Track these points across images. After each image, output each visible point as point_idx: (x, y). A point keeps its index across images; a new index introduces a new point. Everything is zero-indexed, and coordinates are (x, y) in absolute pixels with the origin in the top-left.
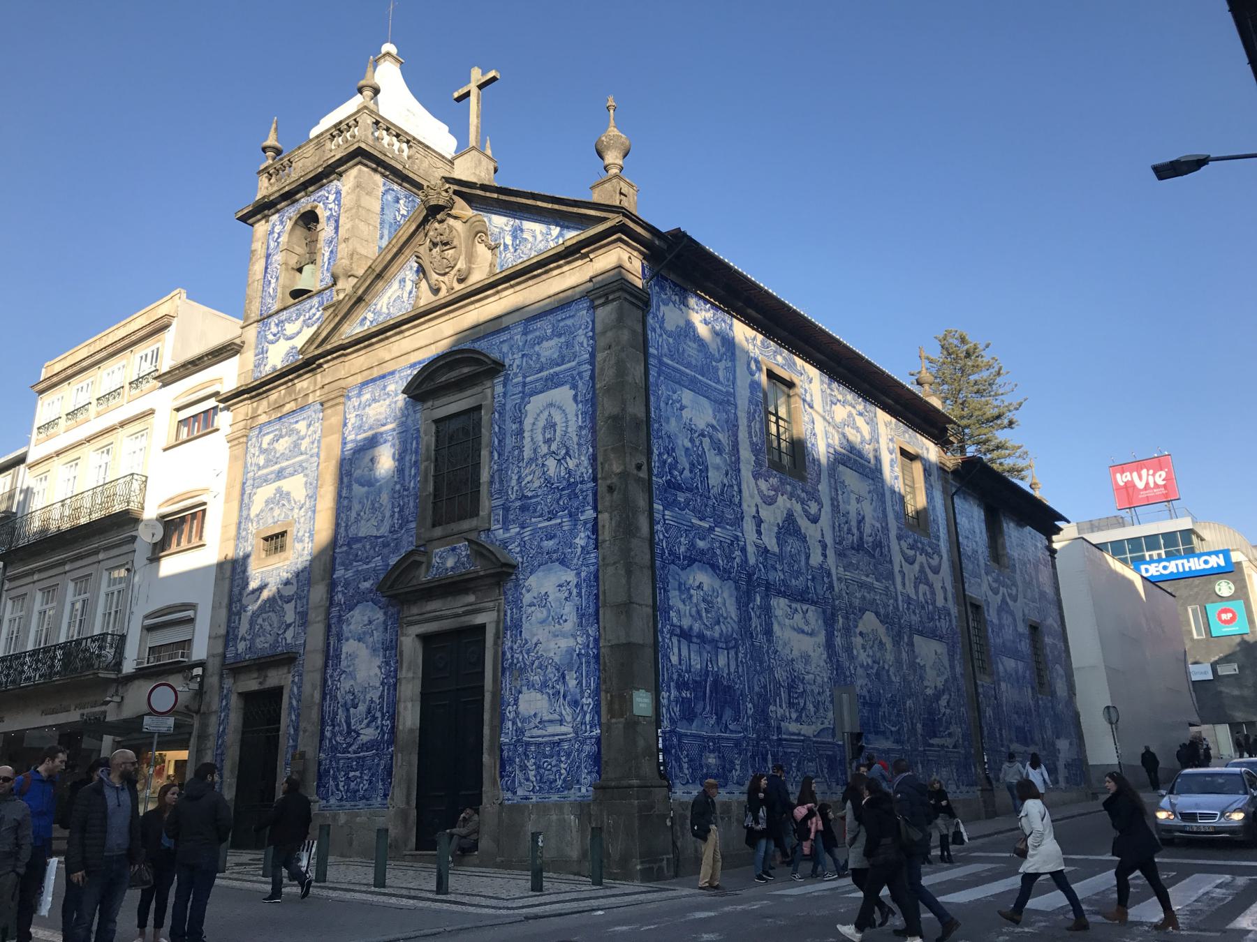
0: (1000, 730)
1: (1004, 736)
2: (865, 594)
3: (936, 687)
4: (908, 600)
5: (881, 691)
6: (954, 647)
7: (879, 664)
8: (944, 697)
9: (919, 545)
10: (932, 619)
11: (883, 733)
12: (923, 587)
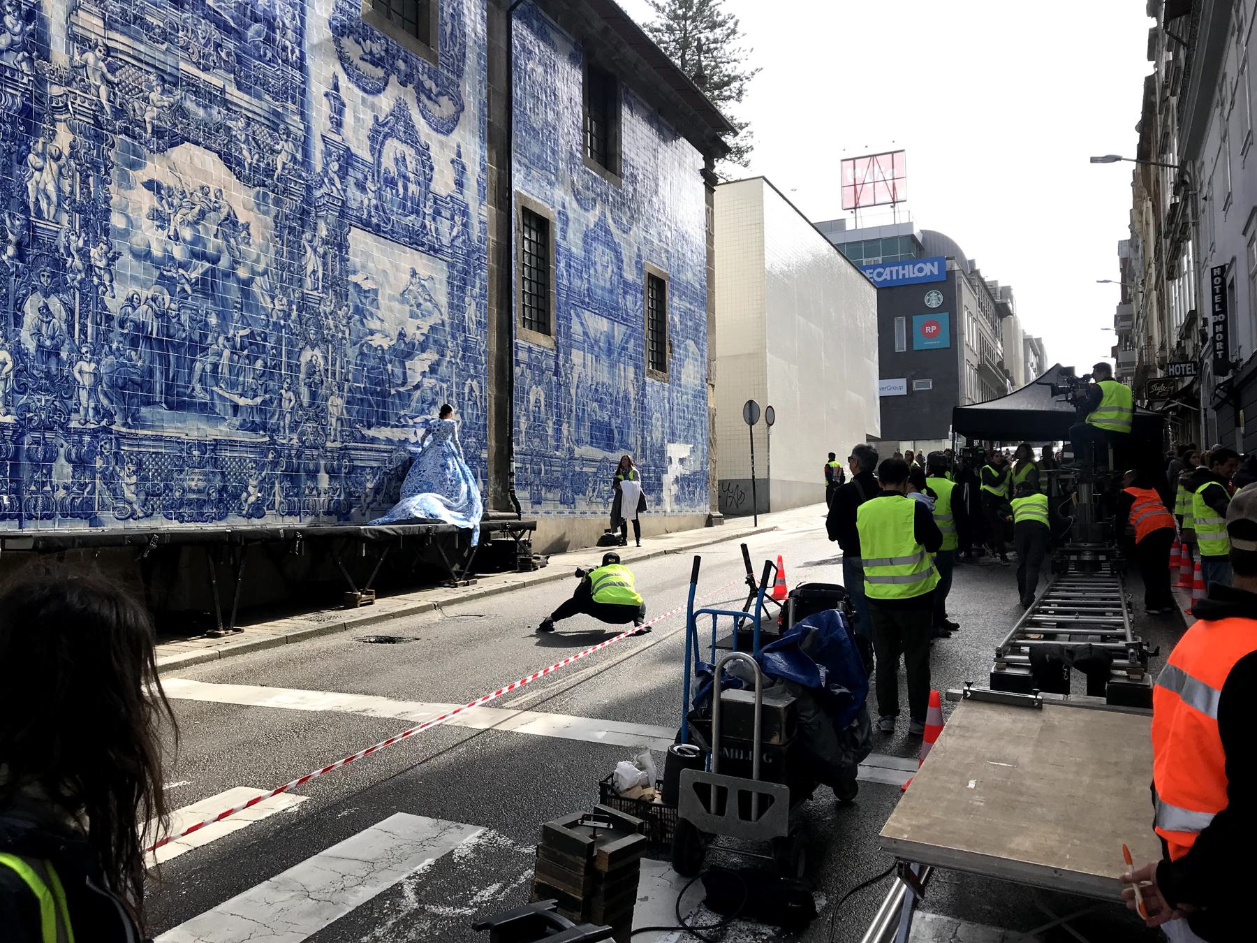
0: (558, 423)
1: (565, 432)
2: (189, 105)
3: (402, 335)
4: (348, 160)
5: (213, 320)
6: (466, 272)
7: (215, 260)
8: (424, 355)
9: (401, 65)
10: (416, 211)
11: (206, 409)
12: (393, 147)
